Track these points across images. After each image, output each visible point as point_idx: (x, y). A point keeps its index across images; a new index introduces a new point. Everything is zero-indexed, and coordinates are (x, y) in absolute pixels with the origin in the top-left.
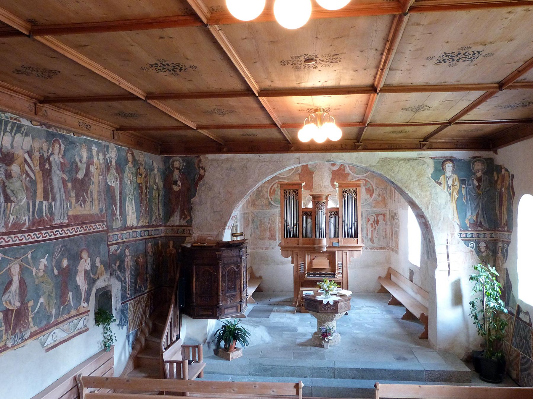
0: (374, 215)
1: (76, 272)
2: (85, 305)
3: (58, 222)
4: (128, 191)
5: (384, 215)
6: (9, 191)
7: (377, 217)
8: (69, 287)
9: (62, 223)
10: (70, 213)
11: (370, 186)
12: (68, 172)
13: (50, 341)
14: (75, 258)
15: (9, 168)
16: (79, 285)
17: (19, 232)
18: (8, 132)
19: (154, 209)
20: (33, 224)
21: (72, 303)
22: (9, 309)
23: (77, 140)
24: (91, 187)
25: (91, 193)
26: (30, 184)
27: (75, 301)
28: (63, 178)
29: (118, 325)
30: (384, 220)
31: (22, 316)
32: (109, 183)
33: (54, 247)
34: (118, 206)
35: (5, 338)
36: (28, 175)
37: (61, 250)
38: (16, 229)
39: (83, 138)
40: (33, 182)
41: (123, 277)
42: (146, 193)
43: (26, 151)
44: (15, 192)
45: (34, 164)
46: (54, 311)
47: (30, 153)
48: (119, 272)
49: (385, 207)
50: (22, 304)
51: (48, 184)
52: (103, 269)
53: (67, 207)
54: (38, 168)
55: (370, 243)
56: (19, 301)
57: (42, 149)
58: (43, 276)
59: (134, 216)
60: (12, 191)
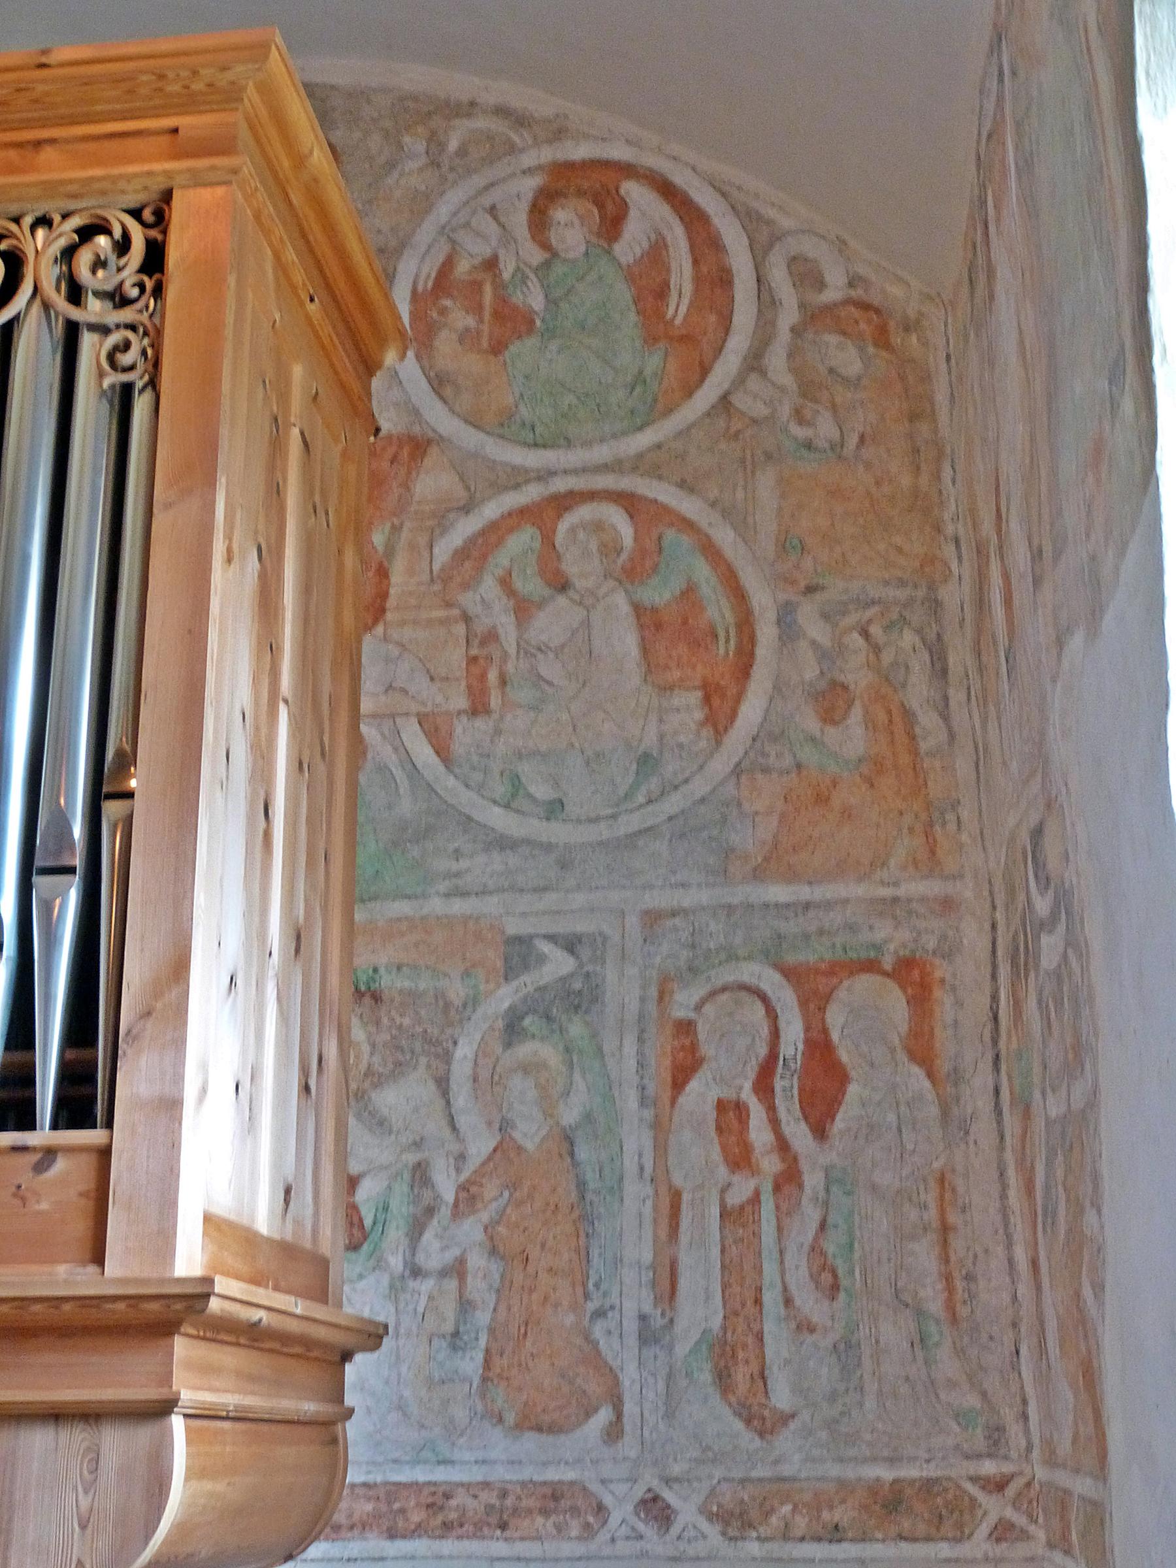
0: (770, 981)
5: (913, 976)
7: (814, 1003)
11: (703, 572)
30: (920, 1049)
49: (929, 861)
55: (717, 1419)
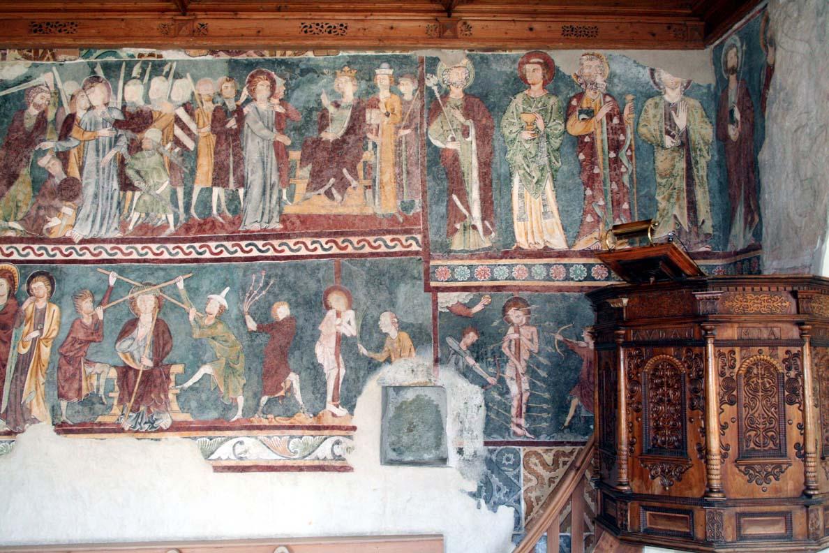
1: (315, 337)
2: (342, 412)
3: (256, 227)
4: (519, 159)
6: (130, 173)
8: (292, 363)
9: (265, 230)
10: (290, 209)
12: (296, 129)
13: (225, 452)
14: (315, 305)
15: (139, 136)
16: (321, 365)
17: (153, 241)
18: (134, 78)
19: (662, 204)
20: (188, 229)
21: (298, 396)
22: (130, 368)
23: (322, 65)
24: (367, 156)
25: (368, 168)
26: (180, 159)
27: (310, 396)
28: (276, 144)
29: (473, 495)
31: (155, 386)
32: (438, 144)
33: (245, 275)
34: (475, 194)
35: (116, 410)
36: (177, 142)
37: (267, 283)
38: (147, 234)
39: (343, 57)
40: (190, 156)
41: (493, 375)
42: (616, 162)
43: (181, 103)
44: (142, 174)
45: (197, 124)
46: (241, 401)
47: (188, 107)
48: (471, 361)
50: (156, 364)
51: (228, 156)
52: (408, 342)
53: (280, 198)
54: (207, 129)
56: (152, 360)
57: (220, 95)
58: (214, 326)
59: (554, 222)
60: (138, 172)
